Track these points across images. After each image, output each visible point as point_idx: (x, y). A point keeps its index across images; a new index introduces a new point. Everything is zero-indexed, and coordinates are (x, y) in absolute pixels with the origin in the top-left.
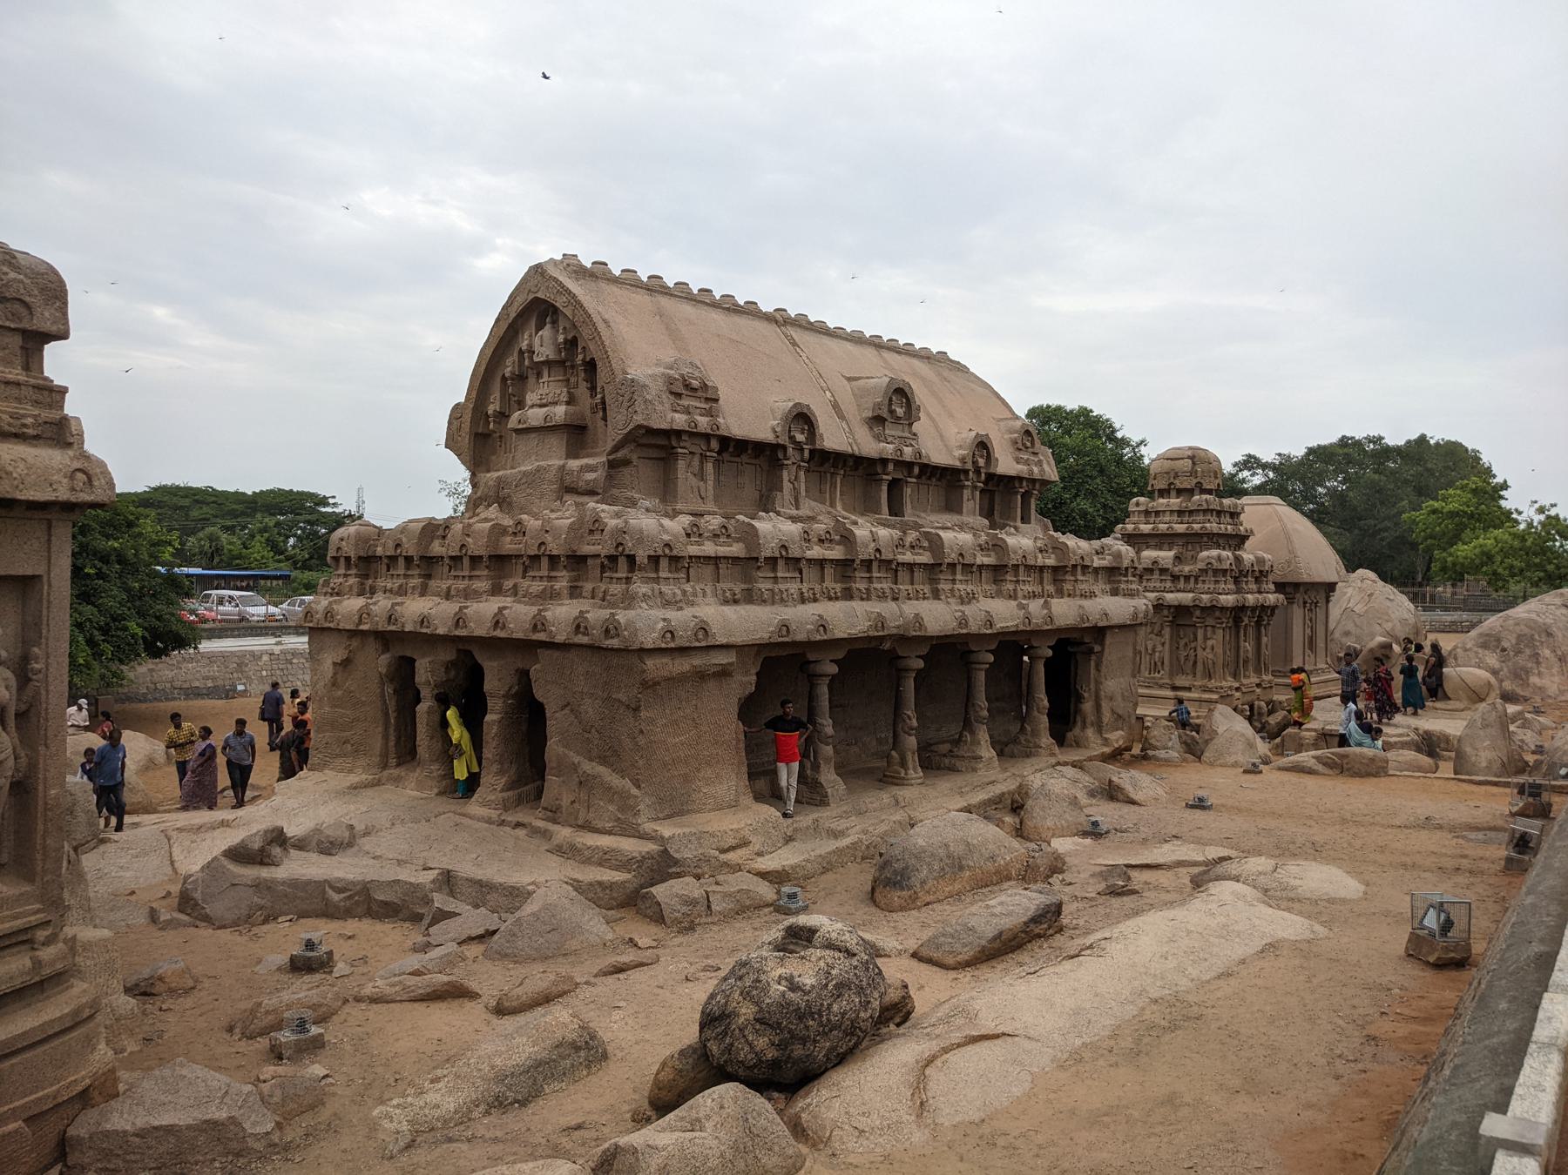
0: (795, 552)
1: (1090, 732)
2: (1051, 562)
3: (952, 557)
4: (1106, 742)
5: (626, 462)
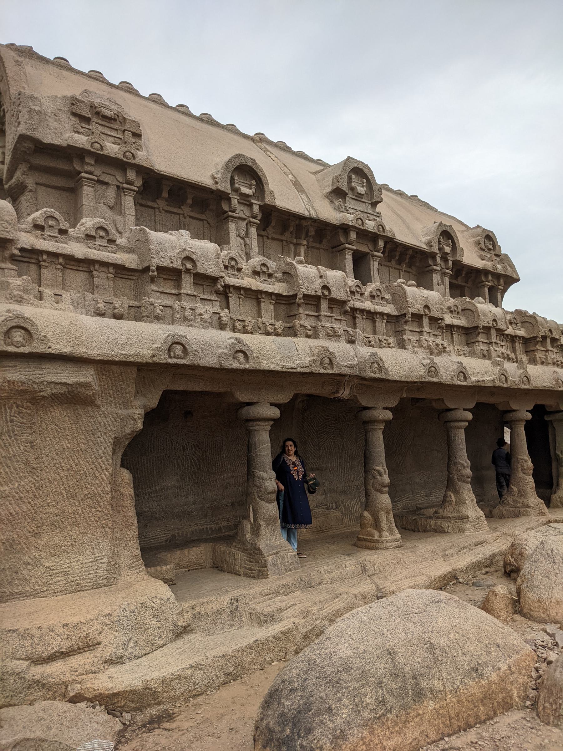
3: (417, 308)
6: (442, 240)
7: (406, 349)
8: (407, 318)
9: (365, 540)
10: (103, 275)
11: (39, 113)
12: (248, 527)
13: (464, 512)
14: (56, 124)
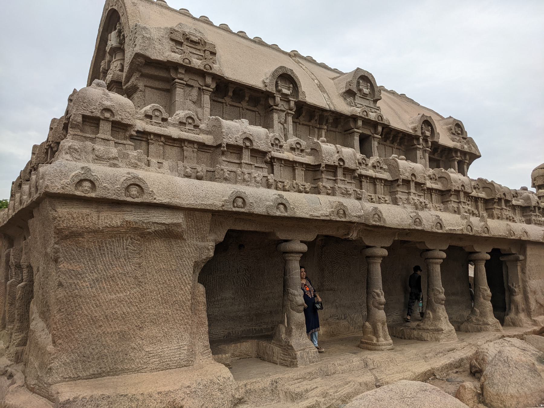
3: (406, 175)
4: (535, 323)
6: (424, 127)
7: (398, 205)
8: (399, 182)
9: (366, 343)
10: (190, 149)
11: (149, 39)
12: (284, 330)
13: (439, 326)
14: (160, 47)
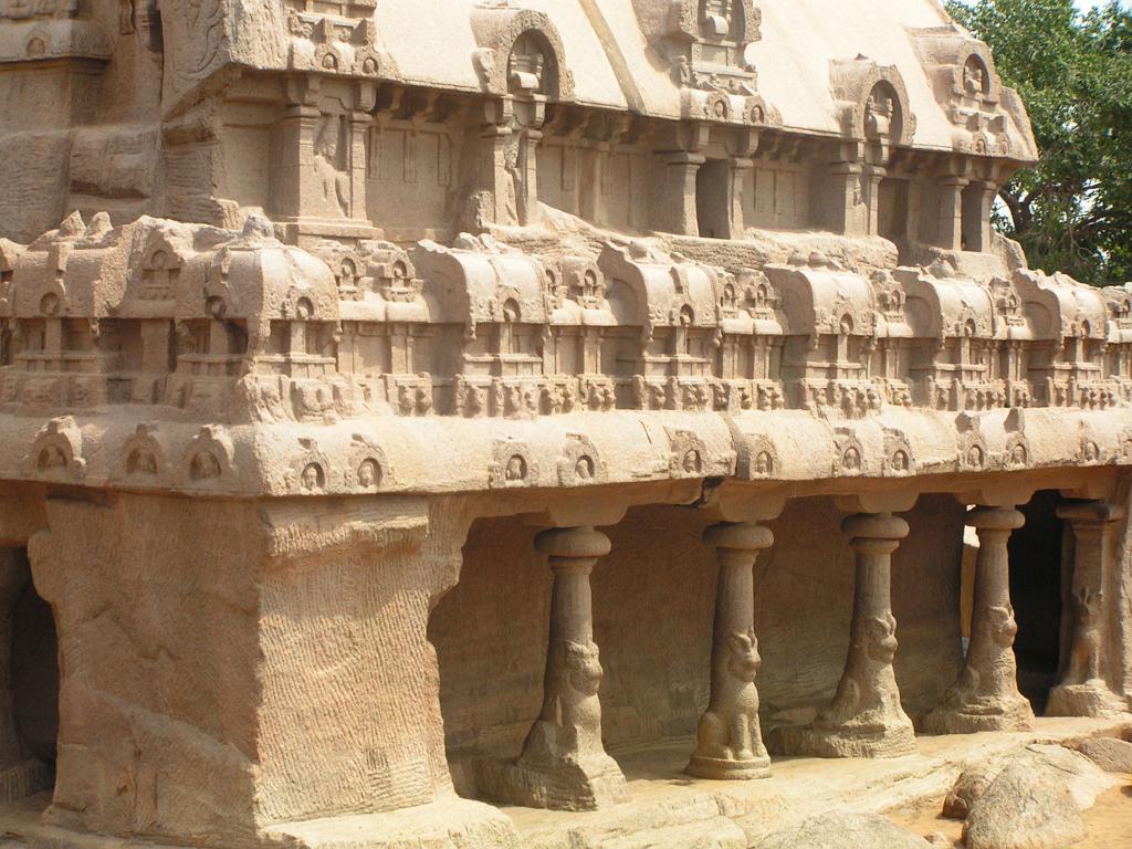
0: (532, 314)
1: (1097, 685)
2: (1022, 331)
5: (205, 136)
13: (876, 719)
